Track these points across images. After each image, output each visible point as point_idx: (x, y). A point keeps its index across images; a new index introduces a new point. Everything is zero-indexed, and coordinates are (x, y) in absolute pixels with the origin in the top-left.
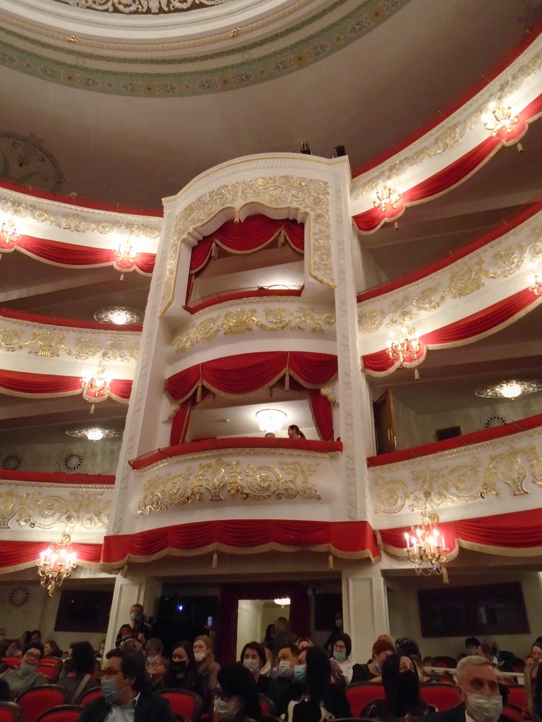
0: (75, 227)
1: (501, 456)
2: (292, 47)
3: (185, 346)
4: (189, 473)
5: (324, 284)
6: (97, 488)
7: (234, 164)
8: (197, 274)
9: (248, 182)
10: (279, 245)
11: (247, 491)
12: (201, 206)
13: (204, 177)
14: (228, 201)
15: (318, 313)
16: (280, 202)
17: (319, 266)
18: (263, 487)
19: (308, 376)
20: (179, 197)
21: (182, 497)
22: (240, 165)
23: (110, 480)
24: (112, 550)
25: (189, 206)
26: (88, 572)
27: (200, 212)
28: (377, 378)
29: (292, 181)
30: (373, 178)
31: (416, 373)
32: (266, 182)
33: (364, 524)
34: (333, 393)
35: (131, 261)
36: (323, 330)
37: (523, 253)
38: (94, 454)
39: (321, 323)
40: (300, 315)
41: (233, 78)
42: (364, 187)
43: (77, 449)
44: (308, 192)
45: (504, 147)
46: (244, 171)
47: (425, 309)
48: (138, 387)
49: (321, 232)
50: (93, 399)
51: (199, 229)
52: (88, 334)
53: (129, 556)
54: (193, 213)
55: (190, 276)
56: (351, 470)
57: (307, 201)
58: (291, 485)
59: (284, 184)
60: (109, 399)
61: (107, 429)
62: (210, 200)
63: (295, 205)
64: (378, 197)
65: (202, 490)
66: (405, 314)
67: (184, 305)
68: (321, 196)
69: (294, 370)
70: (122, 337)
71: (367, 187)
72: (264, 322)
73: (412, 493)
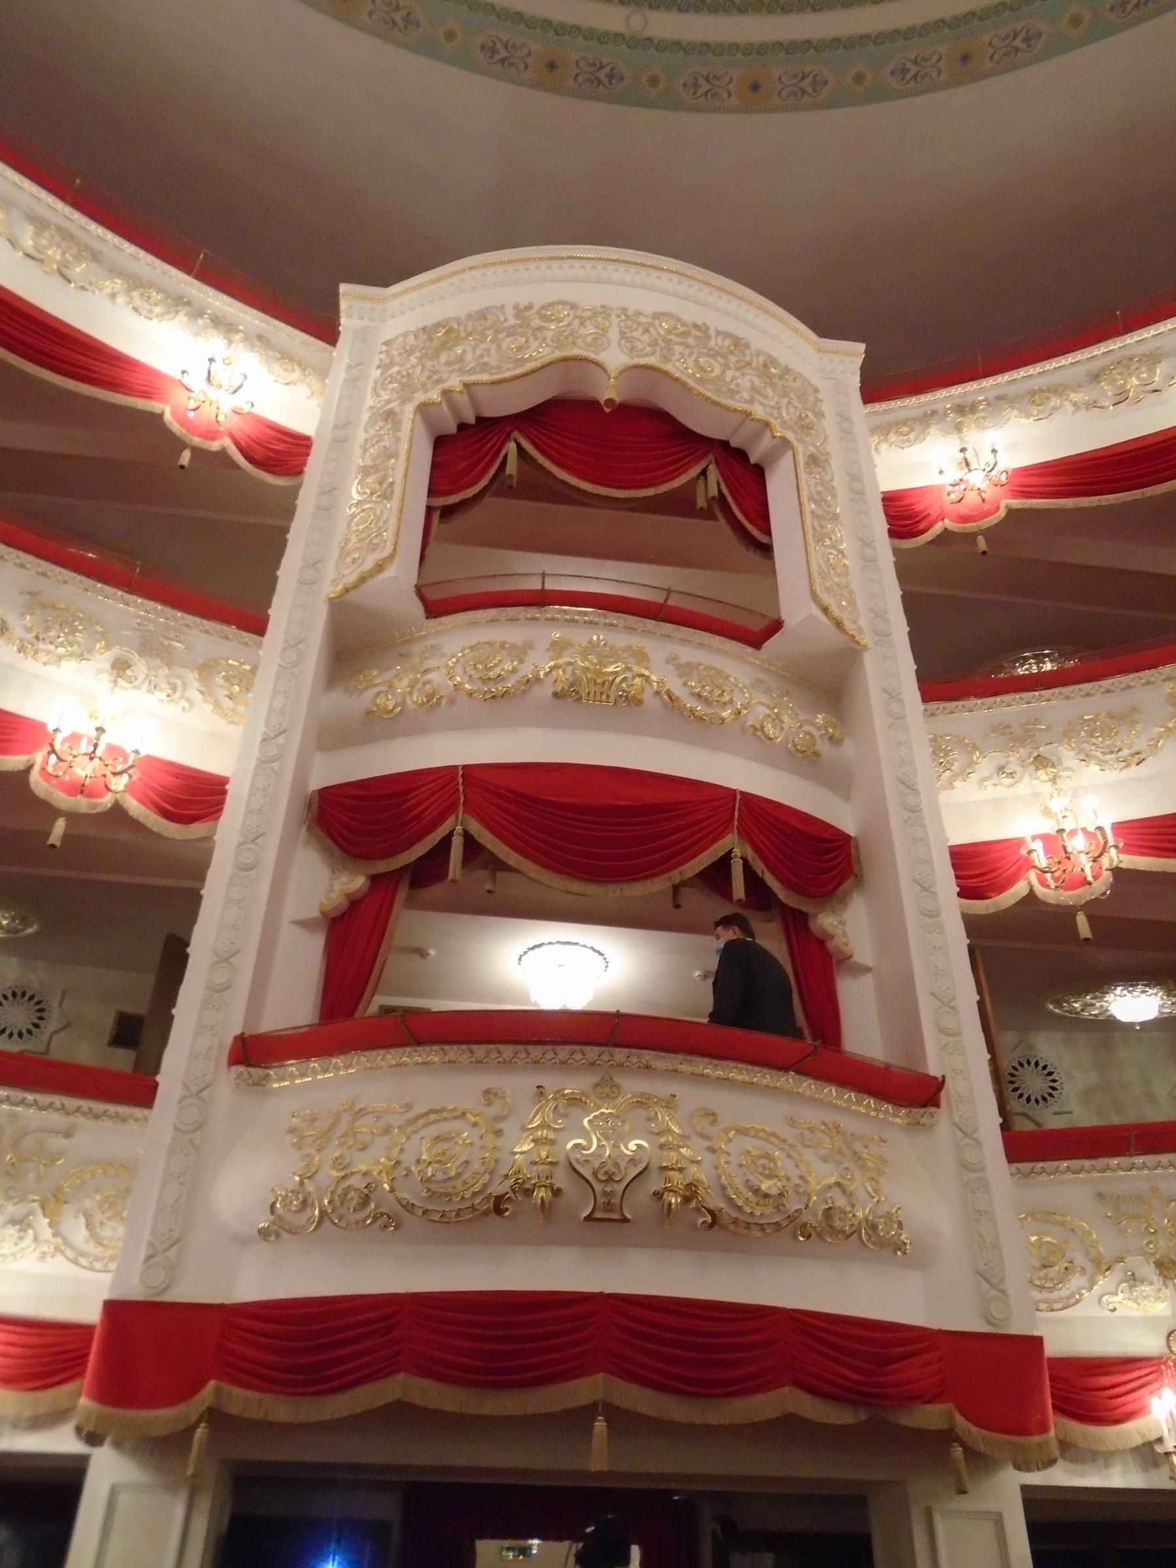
2: (748, 50)
3: (404, 703)
8: (448, 512)
11: (716, 1202)
14: (580, 342)
16: (724, 389)
18: (766, 1196)
20: (395, 296)
21: (475, 1194)
22: (611, 267)
25: (437, 326)
27: (484, 346)
29: (747, 352)
31: (1081, 920)
32: (685, 329)
33: (1037, 1342)
34: (844, 932)
35: (221, 418)
36: (816, 754)
39: (816, 733)
40: (759, 697)
41: (577, 64)
53: (218, 1391)
54: (458, 340)
55: (430, 510)
58: (841, 1201)
59: (731, 353)
60: (117, 812)
63: (759, 411)
65: (561, 1180)
66: (1041, 762)
70: (175, 629)
71: (893, 437)
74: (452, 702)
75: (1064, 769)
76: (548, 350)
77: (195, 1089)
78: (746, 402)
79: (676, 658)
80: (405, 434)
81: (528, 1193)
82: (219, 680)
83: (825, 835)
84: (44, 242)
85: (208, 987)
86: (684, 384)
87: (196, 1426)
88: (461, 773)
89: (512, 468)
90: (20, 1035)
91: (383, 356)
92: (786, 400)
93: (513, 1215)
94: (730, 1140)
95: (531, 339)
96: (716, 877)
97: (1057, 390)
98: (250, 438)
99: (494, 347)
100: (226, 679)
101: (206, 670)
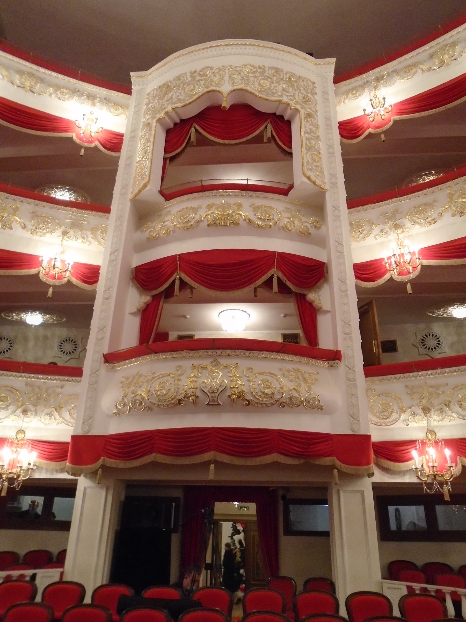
0: (30, 87)
3: (159, 234)
4: (179, 372)
5: (317, 185)
6: (57, 380)
7: (219, 46)
8: (172, 159)
9: (236, 67)
10: (265, 140)
11: (249, 397)
12: (181, 85)
13: (176, 58)
14: (213, 84)
15: (304, 216)
16: (270, 93)
17: (312, 167)
18: (267, 394)
19: (293, 280)
20: (150, 74)
21: (172, 399)
22: (226, 48)
23: (76, 372)
24: (81, 450)
25: (164, 85)
26: (44, 471)
27: (179, 91)
28: (369, 289)
29: (281, 74)
30: (357, 86)
31: (409, 287)
32: (255, 70)
33: (369, 437)
34: (319, 300)
35: (93, 135)
36: (309, 234)
38: (26, 339)
39: (309, 226)
40: (288, 215)
42: (347, 95)
43: (7, 331)
44: (298, 88)
46: (230, 54)
47: (419, 224)
48: (107, 273)
49: (312, 131)
50: (51, 281)
51: (179, 111)
52: (45, 209)
53: (104, 460)
55: (165, 159)
56: (352, 381)
57: (296, 97)
58: (295, 394)
59: (274, 76)
60: (69, 283)
61: (49, 314)
62: (191, 81)
63: (285, 99)
64: (372, 104)
65: (198, 393)
66: (397, 226)
67: (159, 189)
68: (309, 95)
70: (83, 217)
71: (350, 95)
72: (253, 218)
73: (410, 408)
74: (174, 232)
75: (406, 228)
76: (202, 89)
77: (94, 371)
78: (280, 96)
79: (253, 204)
80: (153, 132)
81: (188, 398)
82: (99, 232)
83: (313, 264)
84: (23, 80)
85: (96, 339)
86: (254, 94)
87: (98, 470)
88: (178, 257)
89: (193, 139)
90: (70, 353)
91: (147, 100)
92: (298, 91)
93: (185, 405)
94: (256, 377)
95: (196, 85)
96: (269, 284)
97: (415, 65)
98: (106, 140)
99: (183, 91)
100: (101, 232)
101: (94, 230)
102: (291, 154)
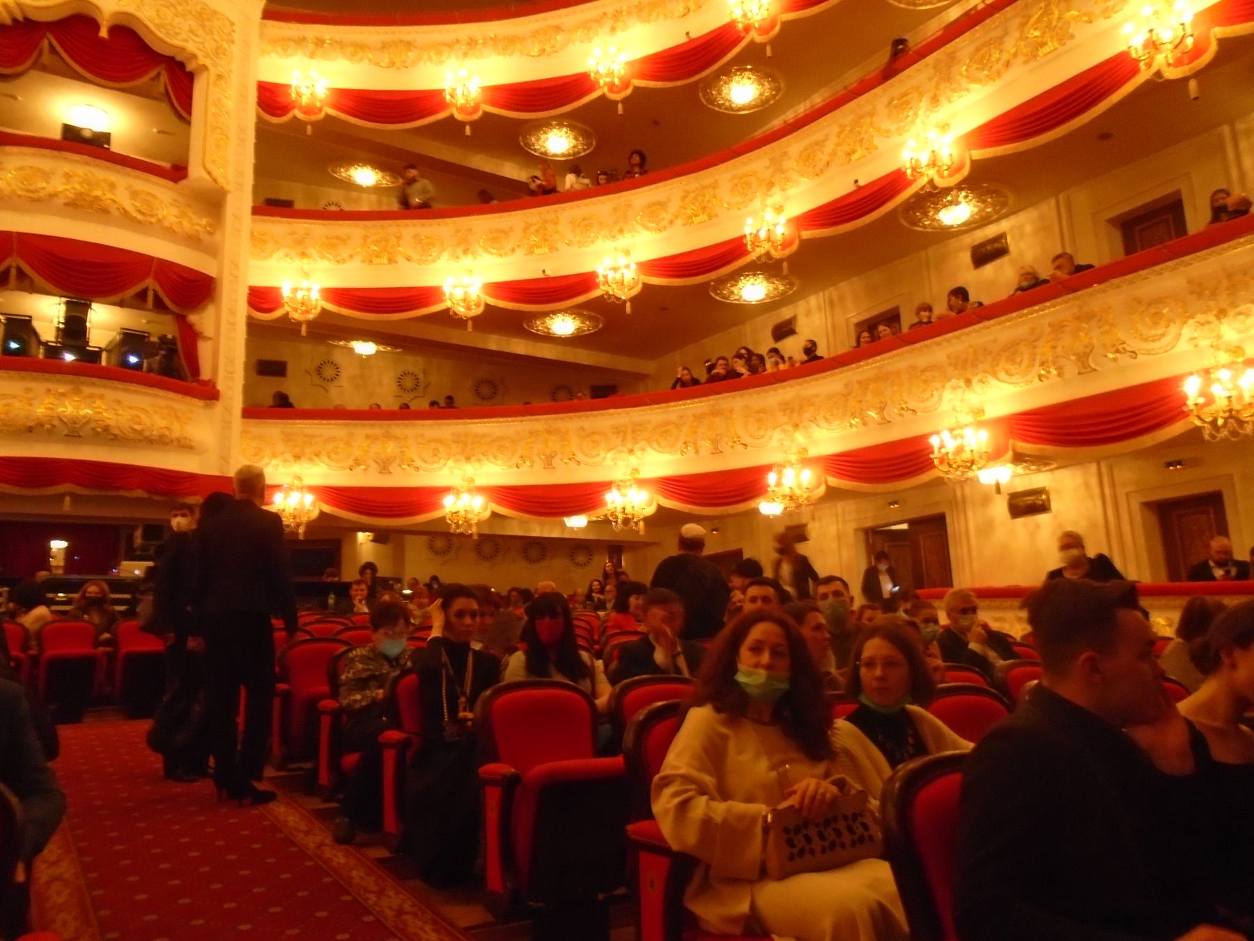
1: (376, 438)
11: (116, 432)
37: (444, 250)
40: (174, 211)
45: (452, 117)
58: (167, 433)
63: (191, 47)
65: (56, 422)
66: (303, 255)
69: (161, 286)
73: (282, 454)
102: (189, 123)
